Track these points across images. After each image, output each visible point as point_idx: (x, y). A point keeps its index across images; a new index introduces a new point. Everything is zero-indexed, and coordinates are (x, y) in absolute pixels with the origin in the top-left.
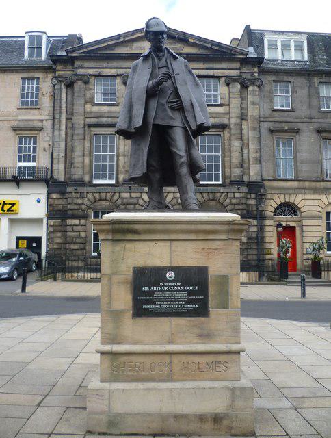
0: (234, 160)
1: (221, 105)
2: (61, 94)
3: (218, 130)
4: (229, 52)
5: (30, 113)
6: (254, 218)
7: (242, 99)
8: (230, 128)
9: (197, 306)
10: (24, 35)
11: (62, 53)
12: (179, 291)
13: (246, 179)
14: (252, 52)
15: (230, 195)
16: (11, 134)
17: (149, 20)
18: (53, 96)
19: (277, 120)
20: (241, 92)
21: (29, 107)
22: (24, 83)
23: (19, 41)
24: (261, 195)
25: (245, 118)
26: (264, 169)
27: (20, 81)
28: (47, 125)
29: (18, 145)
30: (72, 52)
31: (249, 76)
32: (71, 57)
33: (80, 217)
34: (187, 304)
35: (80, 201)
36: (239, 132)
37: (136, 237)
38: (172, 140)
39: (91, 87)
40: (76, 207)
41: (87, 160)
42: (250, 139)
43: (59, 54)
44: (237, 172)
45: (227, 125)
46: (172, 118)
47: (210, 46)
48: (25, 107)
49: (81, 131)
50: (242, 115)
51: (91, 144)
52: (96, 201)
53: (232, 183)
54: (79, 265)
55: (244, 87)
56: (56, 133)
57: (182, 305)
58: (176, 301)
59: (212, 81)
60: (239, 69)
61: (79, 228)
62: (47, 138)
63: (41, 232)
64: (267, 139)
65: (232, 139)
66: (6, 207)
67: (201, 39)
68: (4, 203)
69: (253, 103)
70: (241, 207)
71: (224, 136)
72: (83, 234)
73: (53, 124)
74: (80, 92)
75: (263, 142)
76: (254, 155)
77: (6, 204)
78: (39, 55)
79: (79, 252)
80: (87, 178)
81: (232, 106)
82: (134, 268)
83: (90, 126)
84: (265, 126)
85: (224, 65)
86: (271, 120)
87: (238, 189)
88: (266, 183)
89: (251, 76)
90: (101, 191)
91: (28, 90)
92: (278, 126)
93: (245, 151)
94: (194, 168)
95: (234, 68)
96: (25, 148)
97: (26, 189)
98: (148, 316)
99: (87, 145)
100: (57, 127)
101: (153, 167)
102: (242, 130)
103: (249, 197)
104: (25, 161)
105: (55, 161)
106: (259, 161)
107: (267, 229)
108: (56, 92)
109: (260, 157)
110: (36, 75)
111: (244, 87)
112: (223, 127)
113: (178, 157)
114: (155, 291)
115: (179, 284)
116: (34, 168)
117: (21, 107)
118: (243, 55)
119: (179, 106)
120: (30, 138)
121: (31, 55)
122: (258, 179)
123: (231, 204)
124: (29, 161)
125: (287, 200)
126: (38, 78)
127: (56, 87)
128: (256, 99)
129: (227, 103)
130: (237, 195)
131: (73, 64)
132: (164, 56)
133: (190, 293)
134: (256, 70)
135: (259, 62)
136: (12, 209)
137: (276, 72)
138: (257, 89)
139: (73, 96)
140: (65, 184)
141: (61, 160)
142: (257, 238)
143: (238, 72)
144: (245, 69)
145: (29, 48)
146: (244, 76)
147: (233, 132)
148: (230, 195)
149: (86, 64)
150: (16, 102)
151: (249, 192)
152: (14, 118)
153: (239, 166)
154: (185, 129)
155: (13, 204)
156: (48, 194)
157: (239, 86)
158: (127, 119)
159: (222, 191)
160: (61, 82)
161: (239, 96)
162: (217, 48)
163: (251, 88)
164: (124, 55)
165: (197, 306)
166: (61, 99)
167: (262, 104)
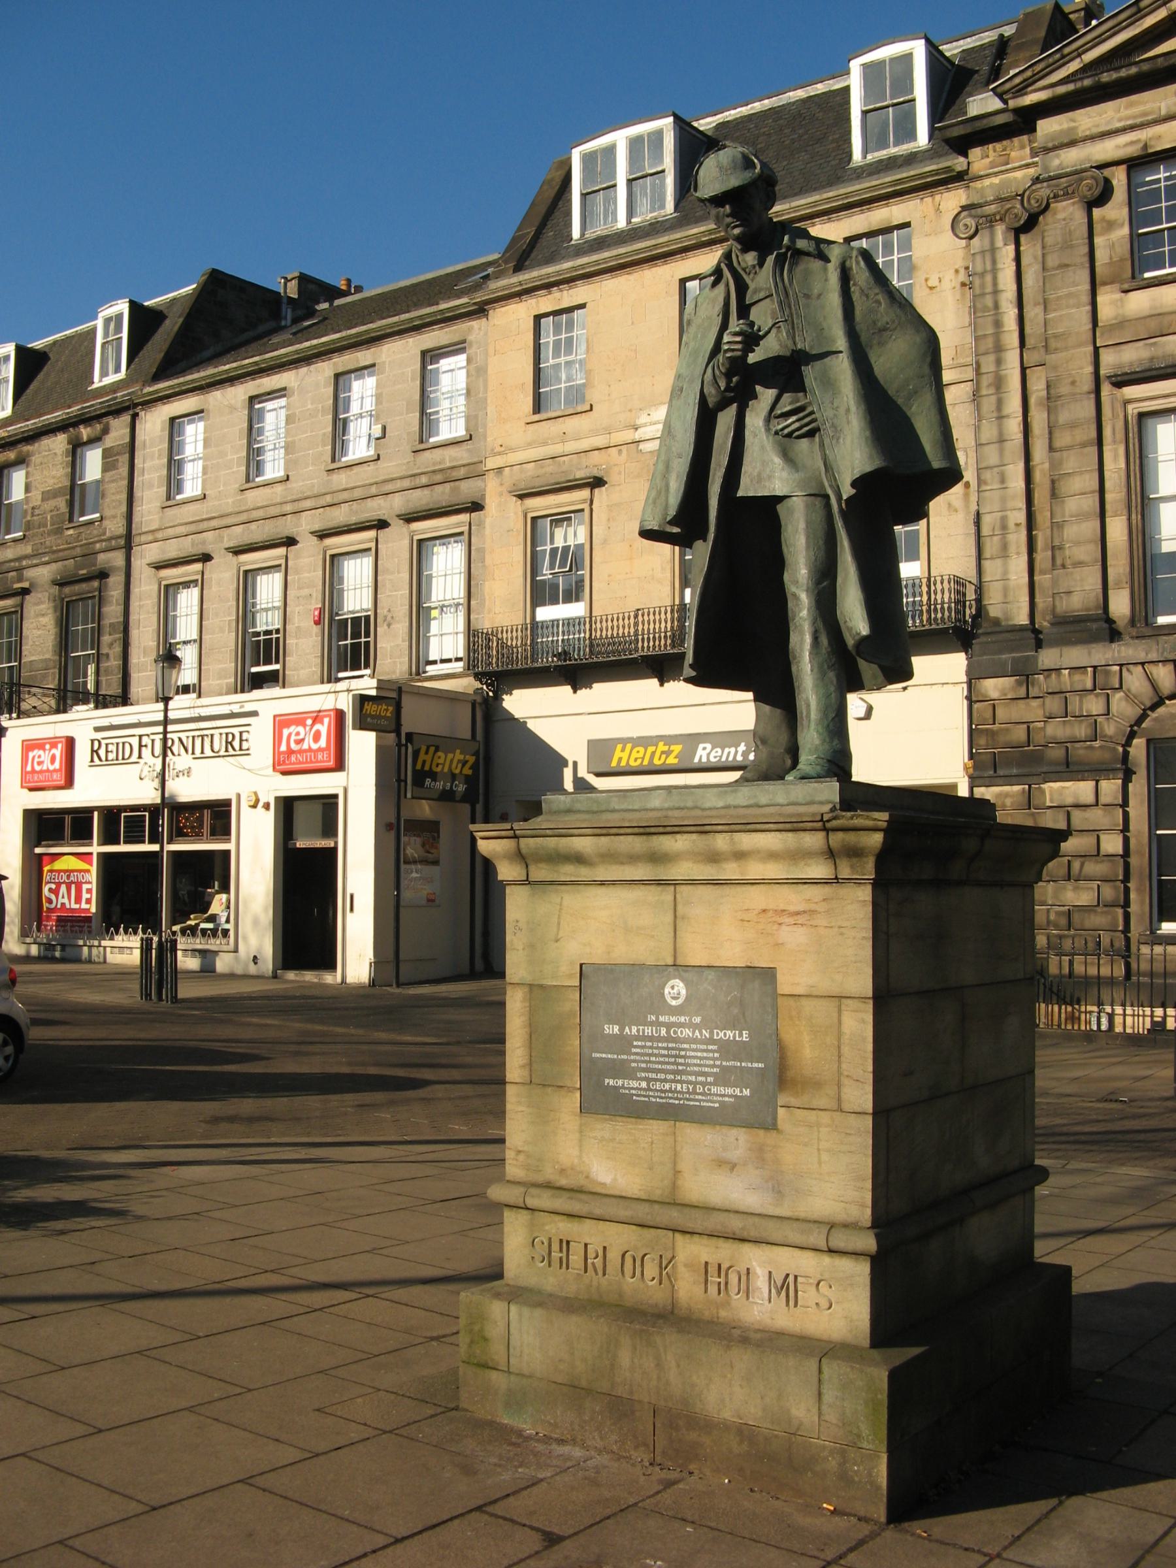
2: (994, 271)
9: (747, 1092)
30: (1021, 90)
32: (1018, 111)
33: (1095, 772)
34: (715, 1084)
35: (1094, 705)
37: (584, 873)
57: (704, 1084)
58: (691, 1073)
74: (1067, 246)
80: (1120, 605)
105: (991, 547)
114: (637, 1038)
115: (698, 1020)
133: (726, 1049)
140: (1035, 637)
141: (1012, 538)
149: (1087, 119)
156: (969, 683)
165: (747, 1092)
166: (996, 292)
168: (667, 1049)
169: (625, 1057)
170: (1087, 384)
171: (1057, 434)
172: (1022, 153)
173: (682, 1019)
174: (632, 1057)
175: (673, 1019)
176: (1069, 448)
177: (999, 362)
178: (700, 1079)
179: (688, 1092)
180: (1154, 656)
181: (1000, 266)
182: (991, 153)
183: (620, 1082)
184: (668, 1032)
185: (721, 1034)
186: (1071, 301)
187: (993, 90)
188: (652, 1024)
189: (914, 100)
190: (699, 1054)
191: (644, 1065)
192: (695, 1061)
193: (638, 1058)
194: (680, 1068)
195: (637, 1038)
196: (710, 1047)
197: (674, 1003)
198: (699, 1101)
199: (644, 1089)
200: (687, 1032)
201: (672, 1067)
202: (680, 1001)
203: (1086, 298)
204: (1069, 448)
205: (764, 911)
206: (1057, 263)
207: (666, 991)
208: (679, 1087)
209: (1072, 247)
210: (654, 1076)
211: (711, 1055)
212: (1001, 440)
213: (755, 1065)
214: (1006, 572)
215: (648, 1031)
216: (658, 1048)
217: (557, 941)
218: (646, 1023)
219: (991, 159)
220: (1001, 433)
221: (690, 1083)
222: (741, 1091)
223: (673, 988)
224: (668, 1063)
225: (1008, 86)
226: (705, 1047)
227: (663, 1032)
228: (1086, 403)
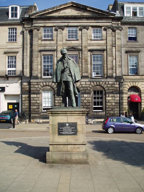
5: (12, 45)
8: (107, 51)
11: (26, 16)
13: (114, 75)
14: (118, 14)
15: (107, 83)
19: (130, 46)
21: (12, 42)
26: (123, 70)
28: (20, 50)
30: (32, 16)
31: (116, 25)
35: (37, 86)
36: (111, 53)
39: (41, 32)
40: (35, 89)
41: (39, 67)
47: (97, 12)
48: (10, 42)
51: (41, 59)
52: (44, 86)
54: (37, 116)
55: (114, 31)
56: (25, 54)
61: (37, 99)
64: (124, 55)
69: (118, 39)
72: (38, 102)
75: (123, 57)
76: (119, 64)
78: (16, 16)
79: (37, 110)
80: (39, 75)
83: (40, 51)
84: (123, 50)
86: (127, 46)
89: (117, 25)
90: (46, 81)
91: (11, 34)
92: (130, 49)
96: (11, 61)
99: (39, 60)
100: (25, 51)
102: (112, 51)
104: (11, 67)
105: (25, 67)
107: (124, 98)
109: (121, 64)
122: (120, 75)
125: (134, 85)
130: (110, 83)
131: (32, 21)
133: (72, 129)
146: (114, 25)
148: (107, 83)
153: (111, 69)
159: (103, 81)
164: (56, 17)
166: (27, 38)
176: (35, 57)
177: (27, 46)
180: (44, 81)
204: (35, 57)
212: (27, 55)
214: (26, 70)
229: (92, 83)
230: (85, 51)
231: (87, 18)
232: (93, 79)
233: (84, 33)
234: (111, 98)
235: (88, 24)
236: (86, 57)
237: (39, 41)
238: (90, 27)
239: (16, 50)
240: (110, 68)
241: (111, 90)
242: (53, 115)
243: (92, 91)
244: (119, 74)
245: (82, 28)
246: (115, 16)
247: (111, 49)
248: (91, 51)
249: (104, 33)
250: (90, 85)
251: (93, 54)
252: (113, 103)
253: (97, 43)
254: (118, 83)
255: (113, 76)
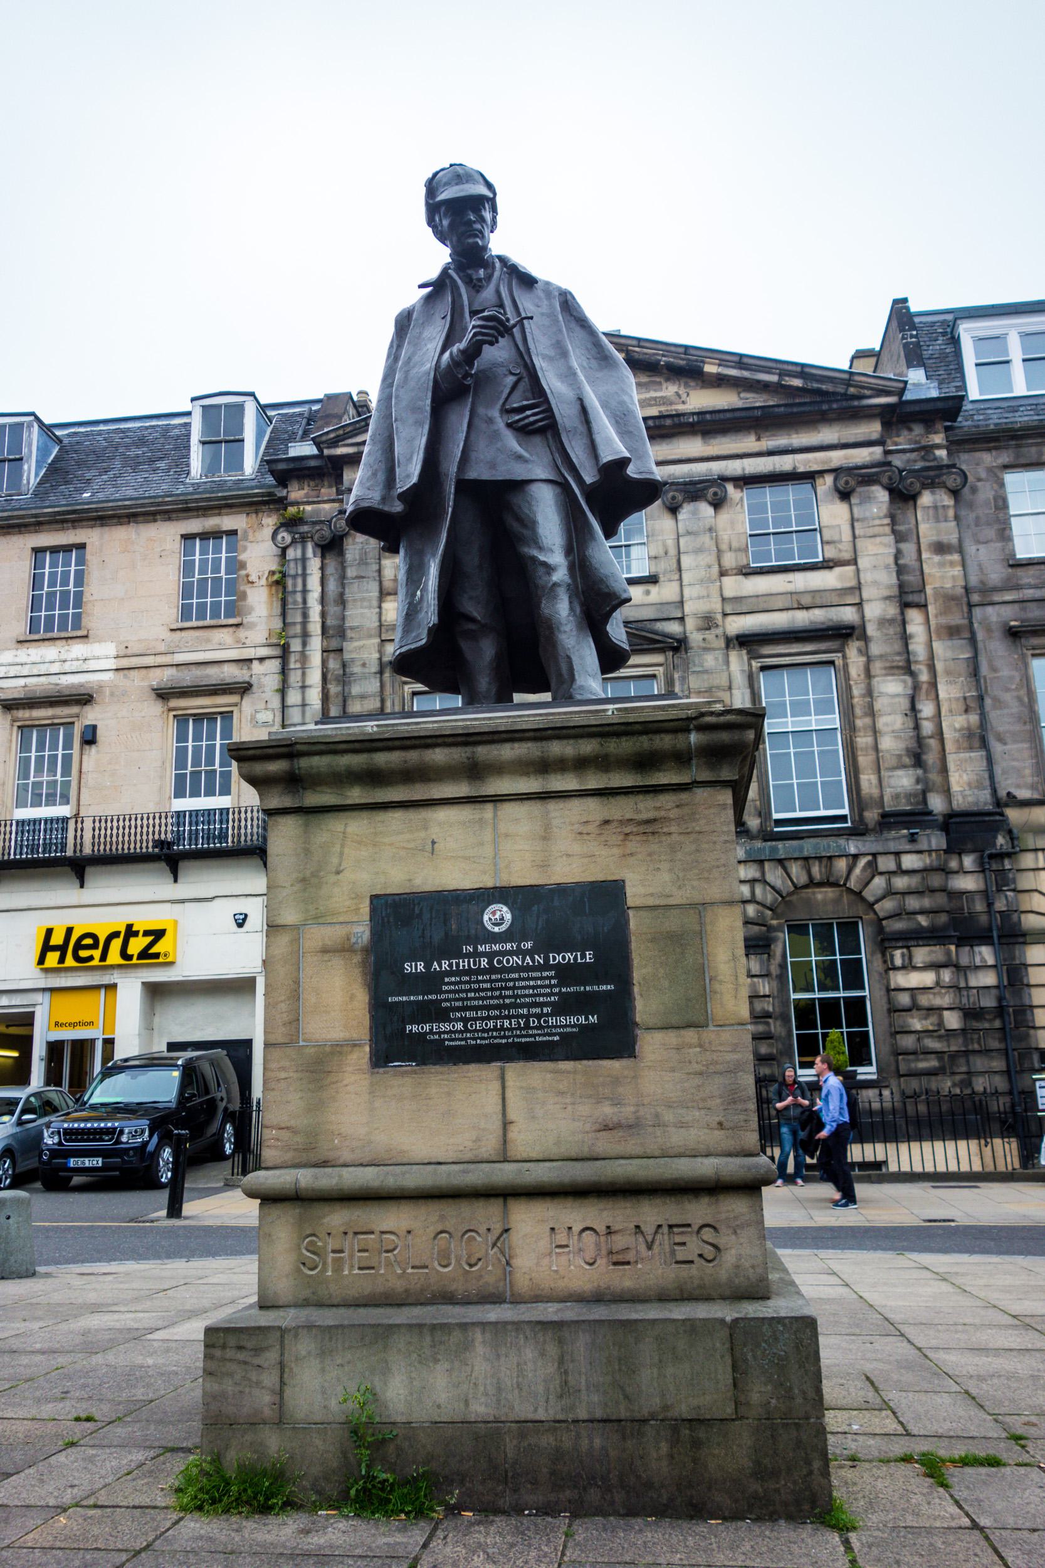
0: (887, 743)
1: (827, 565)
2: (304, 575)
3: (823, 646)
4: (840, 389)
5: (208, 641)
6: (984, 938)
7: (900, 537)
8: (864, 637)
9: (593, 1019)
10: (187, 407)
11: (304, 449)
12: (528, 969)
13: (936, 803)
14: (919, 384)
15: (886, 863)
16: (156, 708)
17: (435, 175)
18: (279, 583)
20: (892, 517)
21: (208, 622)
22: (189, 552)
23: (175, 427)
24: (1001, 856)
25: (910, 598)
27: (176, 545)
28: (266, 675)
29: (172, 745)
30: (335, 443)
32: (331, 458)
34: (551, 1015)
36: (898, 646)
38: (520, 520)
42: (939, 666)
43: (293, 453)
44: (903, 781)
45: (852, 628)
46: (519, 457)
47: (774, 378)
48: (194, 623)
49: (373, 686)
50: (902, 587)
53: (890, 820)
55: (903, 496)
56: (293, 697)
57: (539, 1016)
58: (522, 1006)
59: (791, 493)
60: (880, 442)
62: (265, 716)
63: (249, 1022)
65: (873, 673)
66: (136, 946)
67: (740, 360)
68: (130, 932)
69: (940, 548)
70: (926, 902)
71: (846, 666)
73: (284, 671)
74: (363, 562)
76: (960, 721)
77: (136, 934)
81: (863, 562)
82: (374, 898)
85: (828, 434)
86: (1008, 597)
87: (913, 839)
88: (1014, 815)
93: (927, 709)
94: (597, 601)
95: (860, 439)
96: (197, 750)
97: (199, 881)
98: (423, 1061)
100: (294, 678)
101: (473, 620)
102: (905, 638)
103: (953, 864)
104: (195, 793)
106: (980, 739)
108: (292, 569)
110: (228, 522)
111: (903, 496)
112: (842, 634)
113: (541, 570)
114: (450, 973)
116: (224, 812)
117: (180, 625)
118: (888, 393)
119: (539, 423)
120: (211, 718)
121: (211, 467)
122: (983, 799)
123: (889, 892)
124: (210, 793)
126: (234, 533)
127: (291, 554)
128: (949, 532)
129: (847, 555)
130: (910, 861)
132: (489, 278)
133: (565, 974)
134: (938, 438)
135: (946, 411)
136: (153, 950)
137: (1013, 438)
138: (948, 501)
139: (343, 577)
142: (1000, 1011)
143: (878, 451)
144: (902, 441)
145: (204, 443)
147: (875, 649)
150: (170, 614)
151: (954, 848)
152: (160, 660)
153: (907, 760)
154: (562, 485)
155: (158, 934)
157: (881, 495)
158: (381, 477)
160: (303, 539)
161: (887, 529)
162: (797, 382)
163: (926, 499)
165: (593, 1019)
166: (305, 591)
167: (971, 548)
168: (491, 981)
169: (433, 997)
170: (375, 668)
171: (349, 702)
172: (329, 490)
173: (508, 946)
174: (443, 996)
175: (496, 947)
177: (304, 644)
178: (534, 1010)
179: (519, 1028)
181: (308, 572)
182: (306, 487)
183: (427, 1027)
184: (490, 963)
185: (559, 958)
186: (365, 604)
187: (313, 439)
188: (468, 955)
189: (243, 440)
190: (532, 983)
191: (459, 1004)
192: (527, 992)
193: (451, 996)
194: (507, 1001)
195: (450, 973)
196: (545, 974)
197: (496, 929)
198: (534, 1036)
199: (461, 1032)
200: (516, 960)
201: (496, 1001)
202: (504, 928)
203: (375, 603)
205: (607, 822)
206: (355, 574)
207: (486, 918)
208: (506, 1024)
209: (367, 564)
210: (473, 1014)
211: (547, 982)
213: (604, 987)
215: (464, 964)
216: (478, 982)
217: (338, 873)
218: (460, 955)
219: (305, 491)
220: (303, 699)
221: (522, 1016)
222: (587, 1019)
223: (494, 913)
224: (492, 998)
225: (324, 438)
226: (538, 974)
227: (484, 962)
228: (373, 680)
229: (774, 875)
230: (706, 649)
231: (708, 425)
232: (780, 845)
233: (689, 533)
234: (927, 978)
235: (717, 468)
236: (718, 687)
237: (385, 605)
238: (730, 488)
239: (232, 674)
240: (899, 756)
241: (922, 912)
242: (312, 799)
243: (779, 928)
244: (970, 799)
245: (680, 497)
246: (904, 398)
247: (891, 621)
248: (748, 642)
249: (833, 515)
250: (759, 890)
251: (763, 668)
252: (946, 1013)
253: (790, 588)
254: (968, 861)
255: (930, 813)
